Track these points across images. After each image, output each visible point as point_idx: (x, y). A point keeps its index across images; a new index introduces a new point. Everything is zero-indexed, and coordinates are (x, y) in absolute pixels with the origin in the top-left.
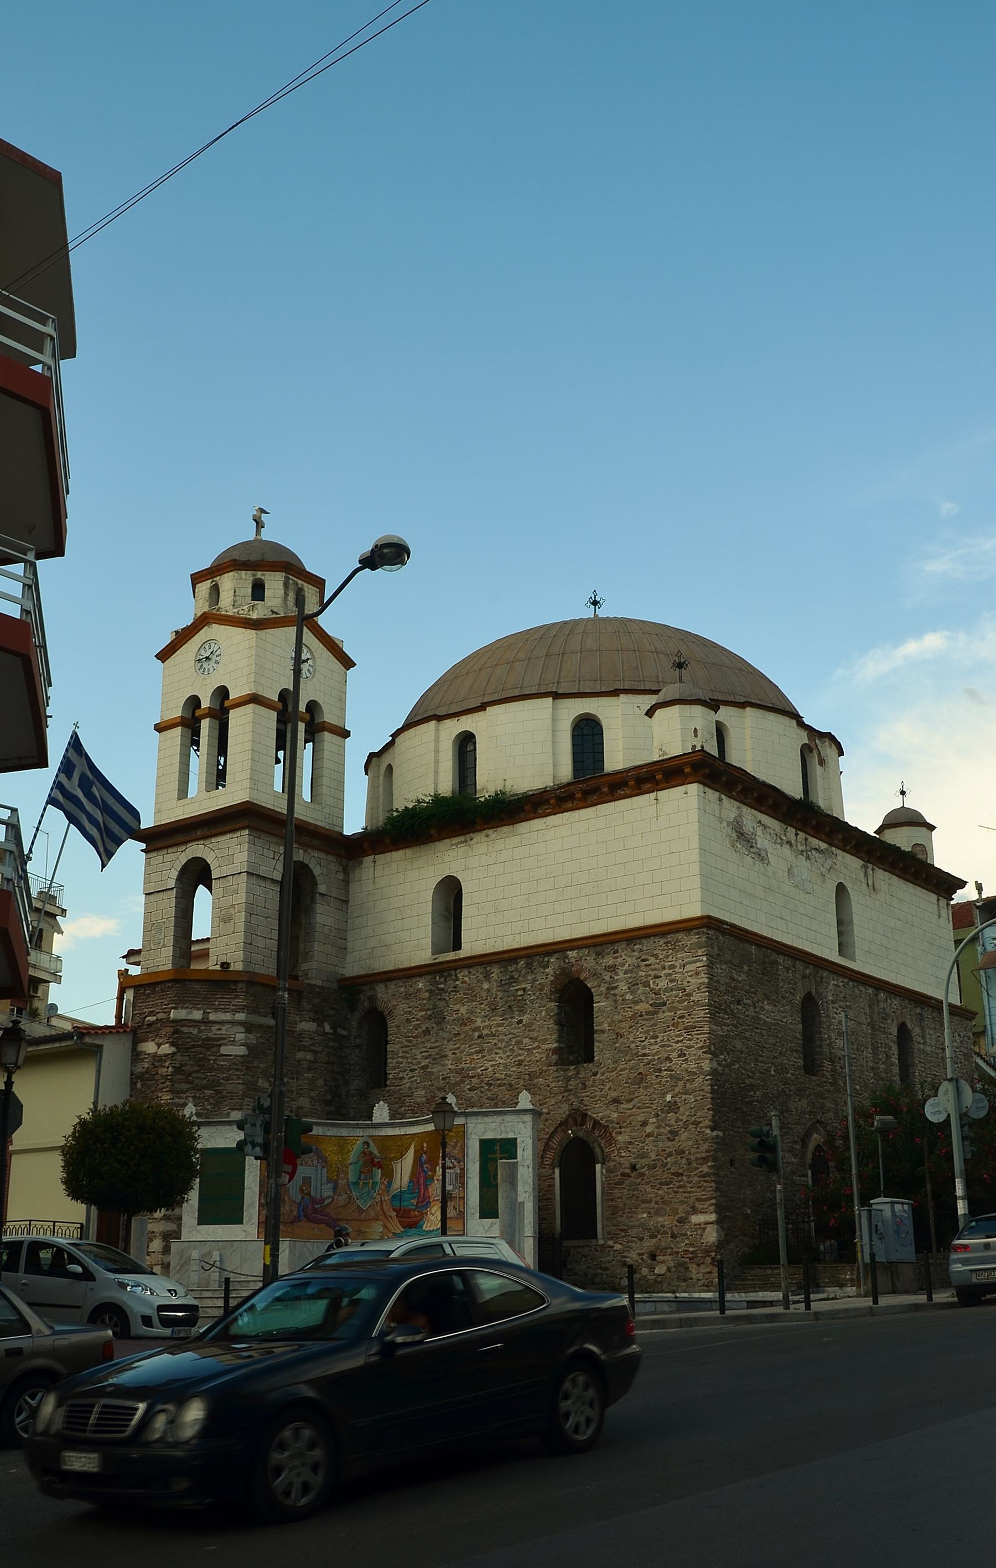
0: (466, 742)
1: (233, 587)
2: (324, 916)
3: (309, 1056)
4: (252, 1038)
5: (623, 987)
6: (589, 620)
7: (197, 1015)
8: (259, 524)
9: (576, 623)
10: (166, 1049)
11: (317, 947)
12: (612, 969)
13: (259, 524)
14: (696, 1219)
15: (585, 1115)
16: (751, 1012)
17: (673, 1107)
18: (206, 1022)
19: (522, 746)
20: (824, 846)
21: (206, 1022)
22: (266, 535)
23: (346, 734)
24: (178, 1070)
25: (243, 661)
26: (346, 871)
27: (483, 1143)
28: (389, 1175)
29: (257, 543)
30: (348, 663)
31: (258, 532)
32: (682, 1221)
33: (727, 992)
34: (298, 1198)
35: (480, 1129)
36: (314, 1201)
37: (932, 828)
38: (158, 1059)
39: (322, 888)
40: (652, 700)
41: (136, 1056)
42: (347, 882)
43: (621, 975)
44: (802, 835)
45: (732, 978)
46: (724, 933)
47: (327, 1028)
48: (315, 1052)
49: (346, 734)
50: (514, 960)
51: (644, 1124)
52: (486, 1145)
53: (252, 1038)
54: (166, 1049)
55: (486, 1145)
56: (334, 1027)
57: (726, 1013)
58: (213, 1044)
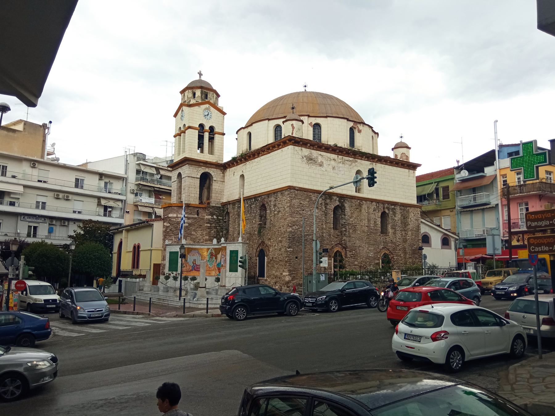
0: (250, 134)
1: (189, 94)
2: (215, 186)
3: (209, 225)
4: (190, 221)
5: (272, 206)
6: (303, 92)
7: (175, 215)
8: (200, 74)
9: (299, 93)
10: (168, 225)
11: (213, 195)
12: (270, 201)
13: (200, 74)
14: (284, 274)
15: (264, 242)
16: (309, 213)
17: (281, 242)
18: (177, 217)
19: (264, 135)
20: (352, 159)
21: (177, 217)
22: (203, 78)
23: (224, 134)
24: (171, 230)
25: (196, 116)
26: (223, 173)
27: (231, 251)
28: (216, 258)
29: (200, 81)
30: (224, 114)
31: (200, 77)
32: (281, 274)
33: (298, 208)
34: (192, 265)
35: (231, 247)
36: (197, 265)
37: (410, 148)
38: (167, 227)
39: (214, 179)
40: (284, 120)
41: (164, 225)
42: (224, 176)
43: (272, 203)
44: (340, 157)
45: (301, 204)
46: (297, 190)
47: (215, 217)
48: (211, 224)
49: (224, 134)
50: (252, 198)
51: (275, 246)
52: (231, 252)
53: (190, 221)
54: (168, 225)
55: (231, 252)
56: (217, 216)
57: (297, 213)
58: (178, 223)
